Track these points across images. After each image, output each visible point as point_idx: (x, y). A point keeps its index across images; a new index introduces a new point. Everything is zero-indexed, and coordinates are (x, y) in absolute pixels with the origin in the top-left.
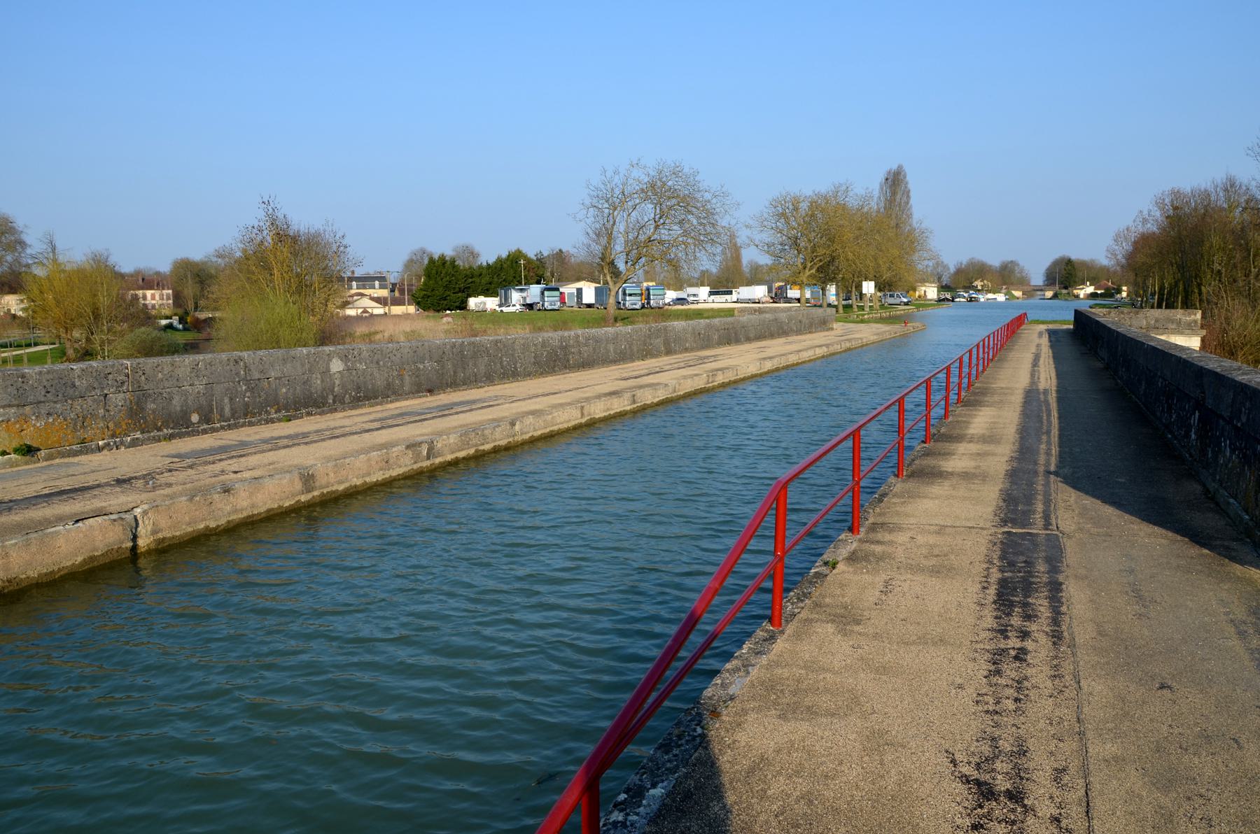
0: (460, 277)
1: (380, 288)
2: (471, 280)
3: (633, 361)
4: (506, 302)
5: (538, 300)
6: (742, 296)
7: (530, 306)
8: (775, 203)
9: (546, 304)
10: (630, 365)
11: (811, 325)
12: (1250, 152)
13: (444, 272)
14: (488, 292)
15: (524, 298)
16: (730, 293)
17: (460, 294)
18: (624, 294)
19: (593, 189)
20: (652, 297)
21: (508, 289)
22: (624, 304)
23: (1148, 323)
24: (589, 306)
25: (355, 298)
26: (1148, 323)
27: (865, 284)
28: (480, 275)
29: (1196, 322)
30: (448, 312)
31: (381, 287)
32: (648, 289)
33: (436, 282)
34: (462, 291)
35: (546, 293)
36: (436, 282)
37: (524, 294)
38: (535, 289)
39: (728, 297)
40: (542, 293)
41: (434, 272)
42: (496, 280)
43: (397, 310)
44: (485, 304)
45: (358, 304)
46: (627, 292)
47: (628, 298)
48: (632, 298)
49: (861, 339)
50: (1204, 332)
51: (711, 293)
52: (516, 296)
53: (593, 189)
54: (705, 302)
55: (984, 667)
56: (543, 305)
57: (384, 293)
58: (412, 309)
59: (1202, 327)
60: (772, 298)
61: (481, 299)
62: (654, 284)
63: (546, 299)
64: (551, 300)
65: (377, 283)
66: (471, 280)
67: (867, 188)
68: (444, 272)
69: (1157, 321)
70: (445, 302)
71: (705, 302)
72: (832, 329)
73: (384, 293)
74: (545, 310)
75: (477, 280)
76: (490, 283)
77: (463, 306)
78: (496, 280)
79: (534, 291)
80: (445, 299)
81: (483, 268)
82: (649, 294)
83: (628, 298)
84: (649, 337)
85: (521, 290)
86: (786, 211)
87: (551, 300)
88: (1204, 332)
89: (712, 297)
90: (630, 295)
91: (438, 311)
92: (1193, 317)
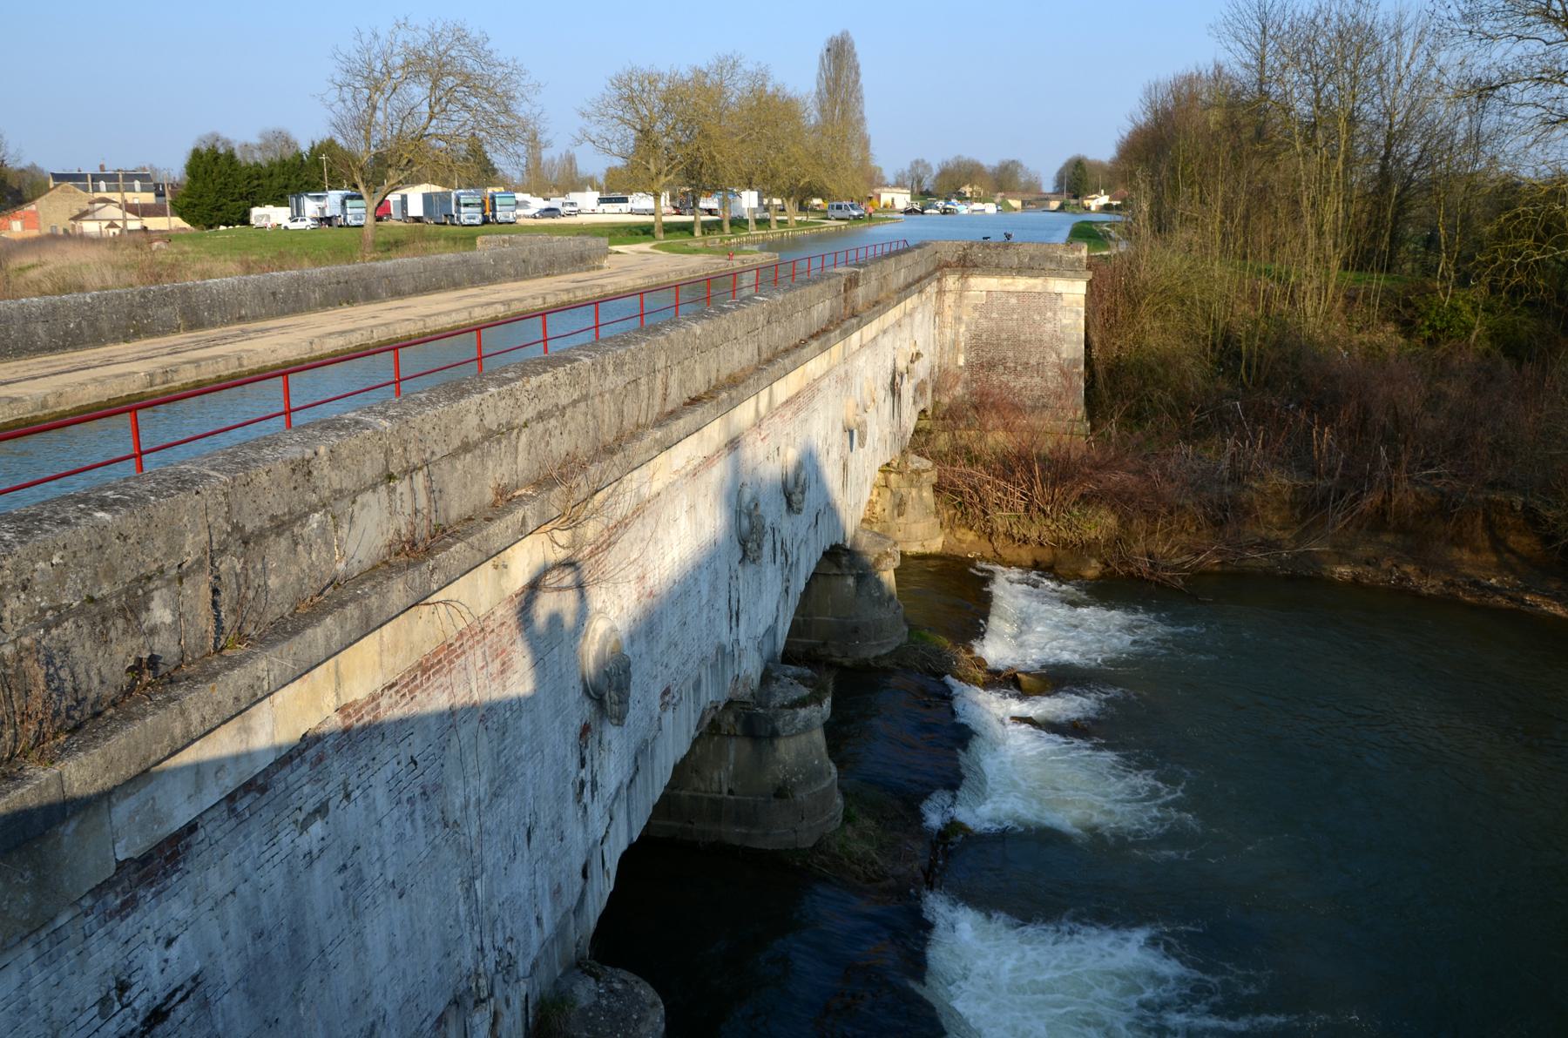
0: (240, 178)
1: (142, 191)
2: (256, 182)
3: (104, 344)
4: (297, 215)
5: (337, 212)
6: (637, 206)
7: (328, 220)
8: (621, 83)
9: (349, 218)
10: (61, 356)
11: (551, 264)
12: (1211, 30)
13: (216, 171)
14: (280, 201)
15: (322, 210)
16: (625, 200)
17: (241, 203)
18: (458, 204)
19: (343, 59)
20: (498, 208)
21: (300, 197)
22: (458, 218)
23: (1021, 262)
24: (417, 219)
25: (98, 205)
26: (1021, 262)
27: (754, 195)
28: (271, 175)
29: (1080, 260)
30: (222, 228)
31: (144, 189)
32: (493, 198)
33: (205, 186)
34: (242, 197)
35: (349, 203)
36: (205, 186)
37: (321, 204)
38: (334, 196)
39: (622, 206)
40: (343, 203)
41: (201, 170)
42: (293, 181)
43: (154, 223)
44: (268, 217)
45: (98, 215)
46: (462, 201)
47: (463, 209)
48: (469, 209)
49: (602, 286)
50: (1090, 275)
51: (602, 201)
52: (311, 207)
53: (343, 59)
54: (593, 212)
55: (566, 834)
56: (345, 219)
57: (149, 198)
58: (178, 222)
59: (1089, 268)
60: (675, 208)
61: (269, 209)
62: (502, 189)
63: (349, 211)
64: (358, 213)
65: (137, 184)
66: (256, 182)
67: (759, 63)
68: (216, 171)
69: (1032, 258)
70: (220, 214)
71: (593, 212)
72: (600, 268)
73: (149, 198)
74: (348, 226)
75: (265, 182)
76: (286, 187)
77: (245, 221)
78: (293, 181)
79: (332, 201)
80: (219, 209)
81: (275, 165)
82: (494, 204)
83: (463, 209)
84: (143, 306)
85: (318, 198)
86: (631, 92)
87: (358, 213)
88: (1090, 275)
89: (603, 206)
90: (466, 205)
91: (211, 227)
92: (1077, 253)
